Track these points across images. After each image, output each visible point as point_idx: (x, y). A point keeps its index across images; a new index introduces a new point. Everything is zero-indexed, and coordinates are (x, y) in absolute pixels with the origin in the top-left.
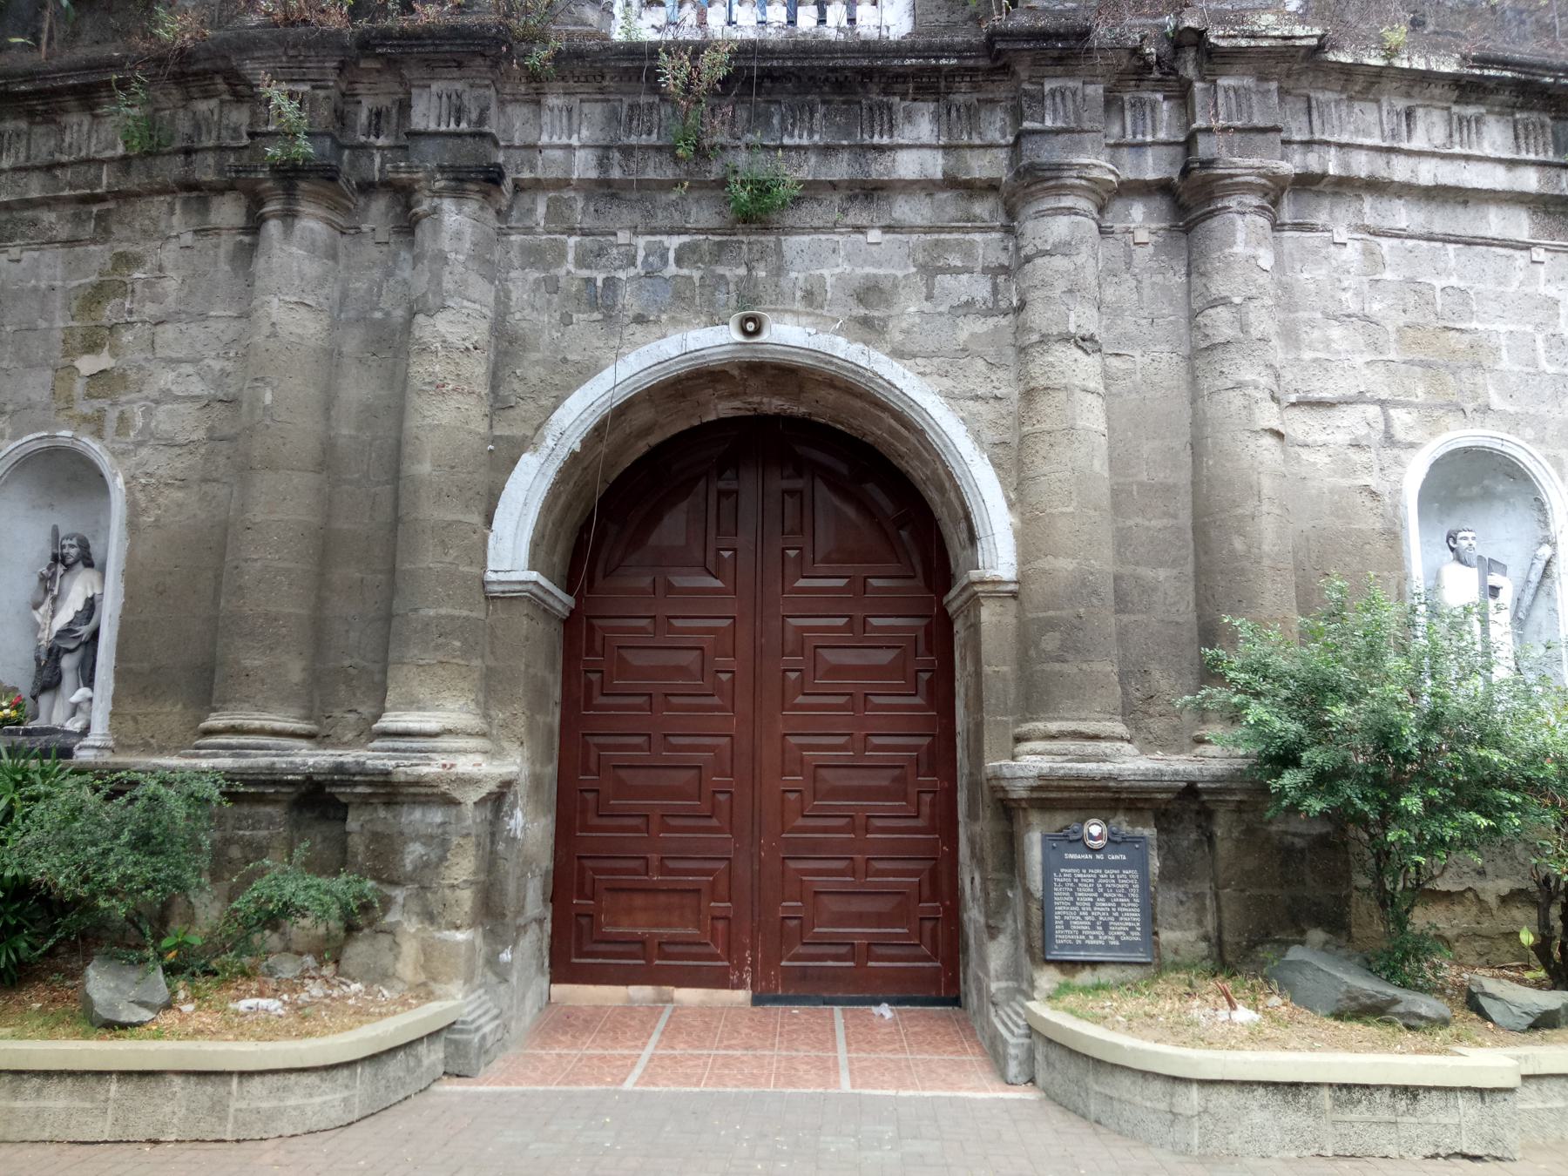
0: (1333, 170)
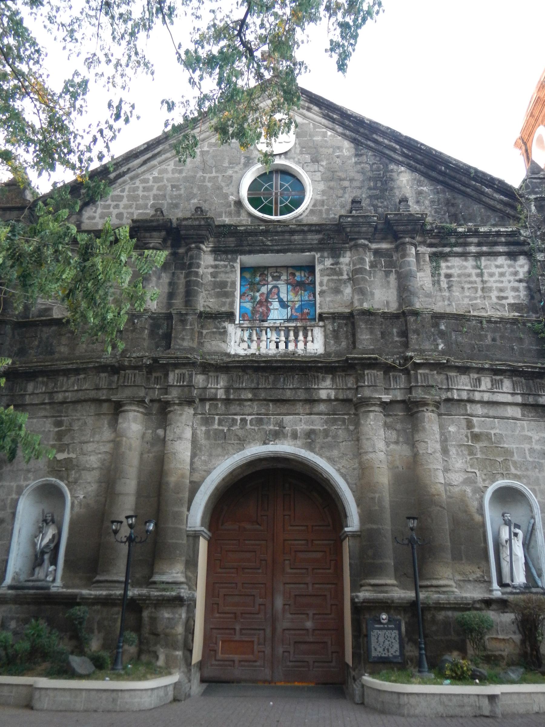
0: (456, 397)
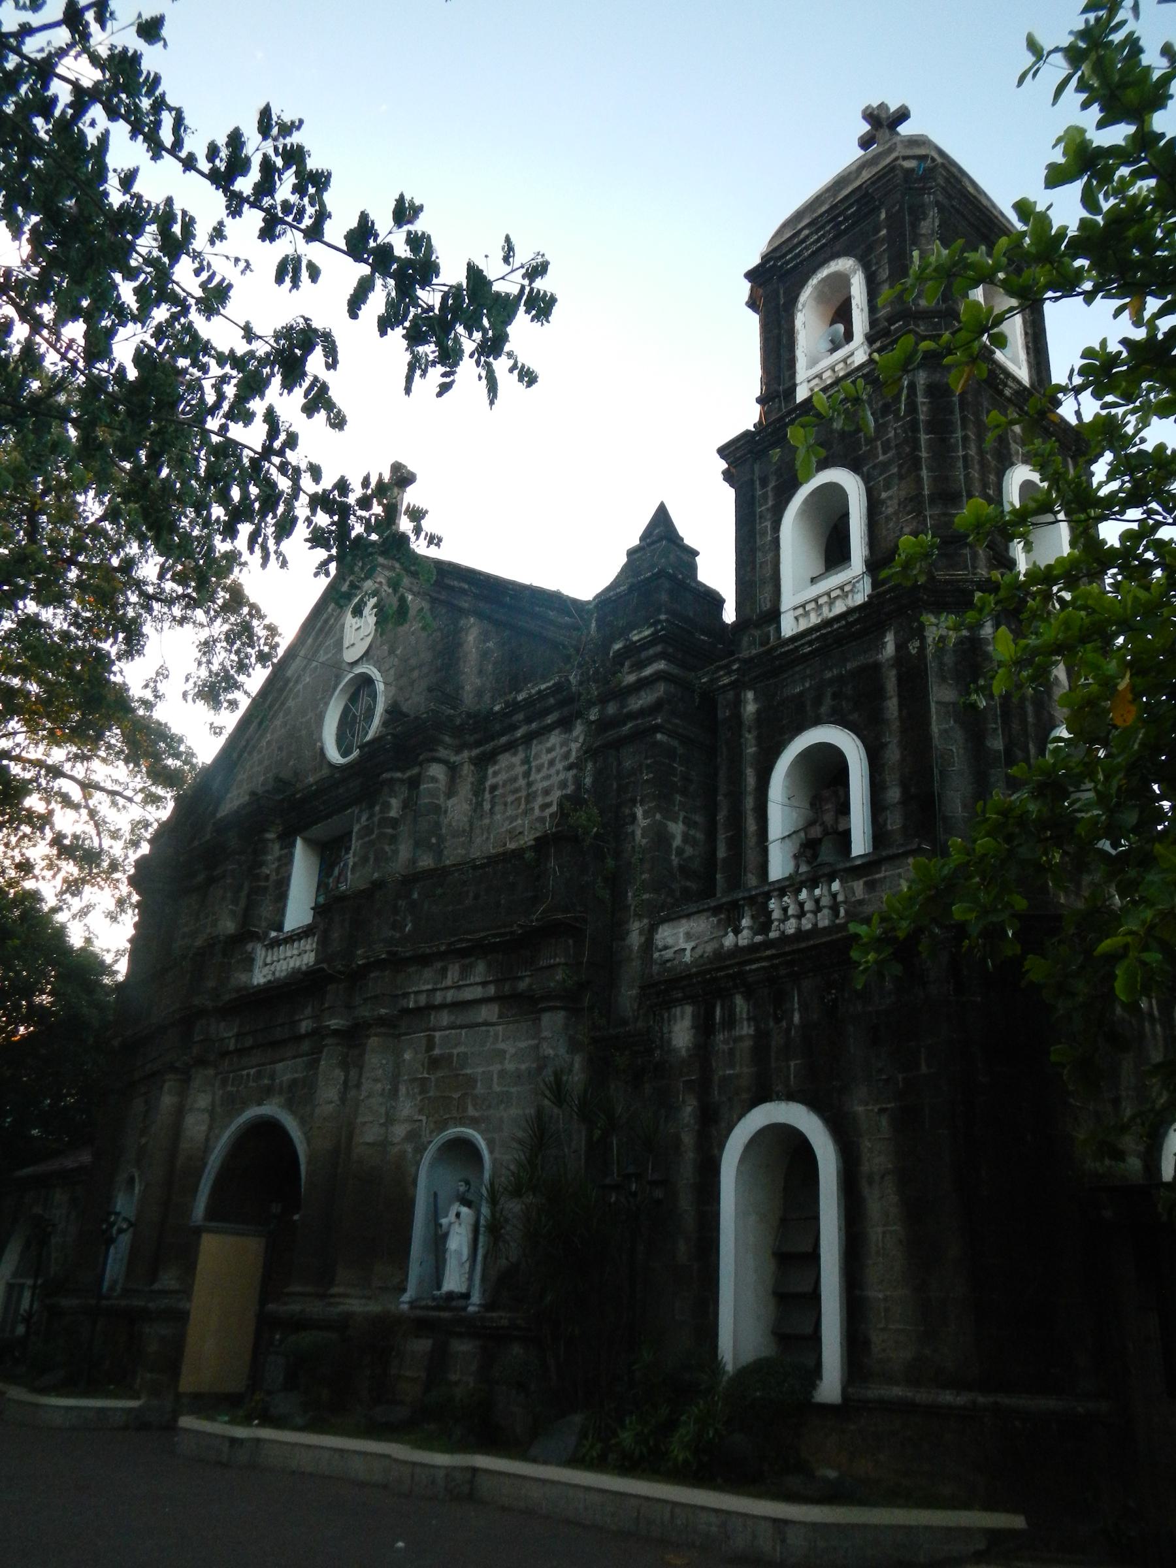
0: (411, 1005)
